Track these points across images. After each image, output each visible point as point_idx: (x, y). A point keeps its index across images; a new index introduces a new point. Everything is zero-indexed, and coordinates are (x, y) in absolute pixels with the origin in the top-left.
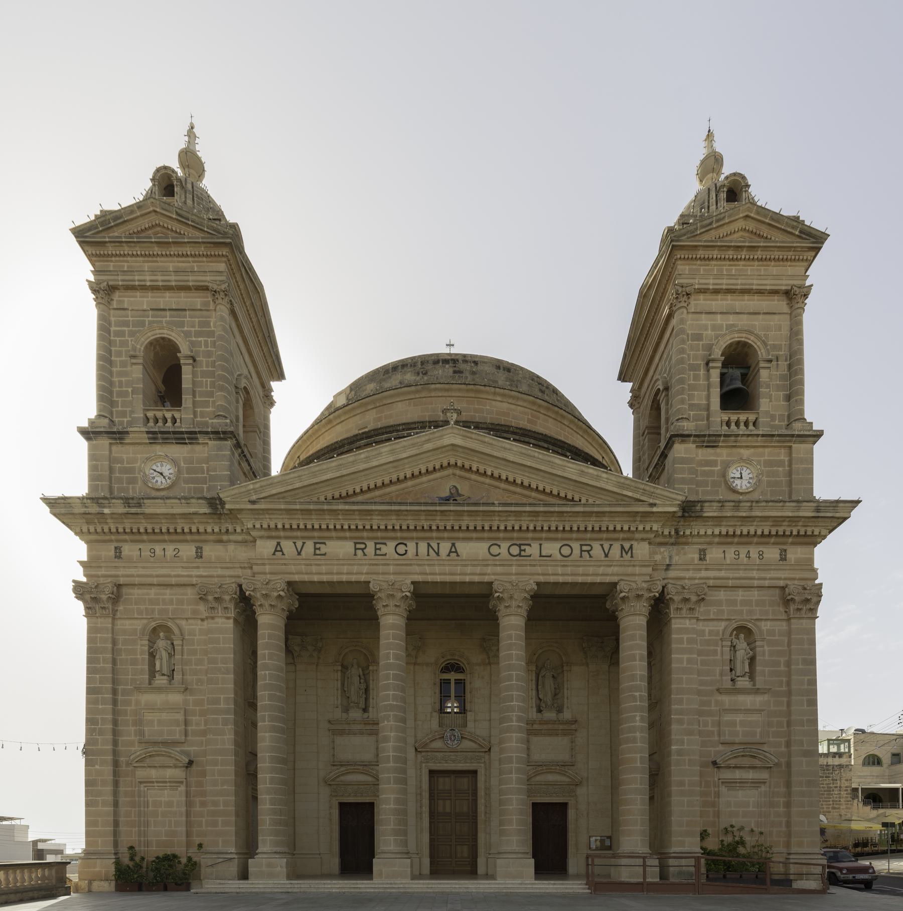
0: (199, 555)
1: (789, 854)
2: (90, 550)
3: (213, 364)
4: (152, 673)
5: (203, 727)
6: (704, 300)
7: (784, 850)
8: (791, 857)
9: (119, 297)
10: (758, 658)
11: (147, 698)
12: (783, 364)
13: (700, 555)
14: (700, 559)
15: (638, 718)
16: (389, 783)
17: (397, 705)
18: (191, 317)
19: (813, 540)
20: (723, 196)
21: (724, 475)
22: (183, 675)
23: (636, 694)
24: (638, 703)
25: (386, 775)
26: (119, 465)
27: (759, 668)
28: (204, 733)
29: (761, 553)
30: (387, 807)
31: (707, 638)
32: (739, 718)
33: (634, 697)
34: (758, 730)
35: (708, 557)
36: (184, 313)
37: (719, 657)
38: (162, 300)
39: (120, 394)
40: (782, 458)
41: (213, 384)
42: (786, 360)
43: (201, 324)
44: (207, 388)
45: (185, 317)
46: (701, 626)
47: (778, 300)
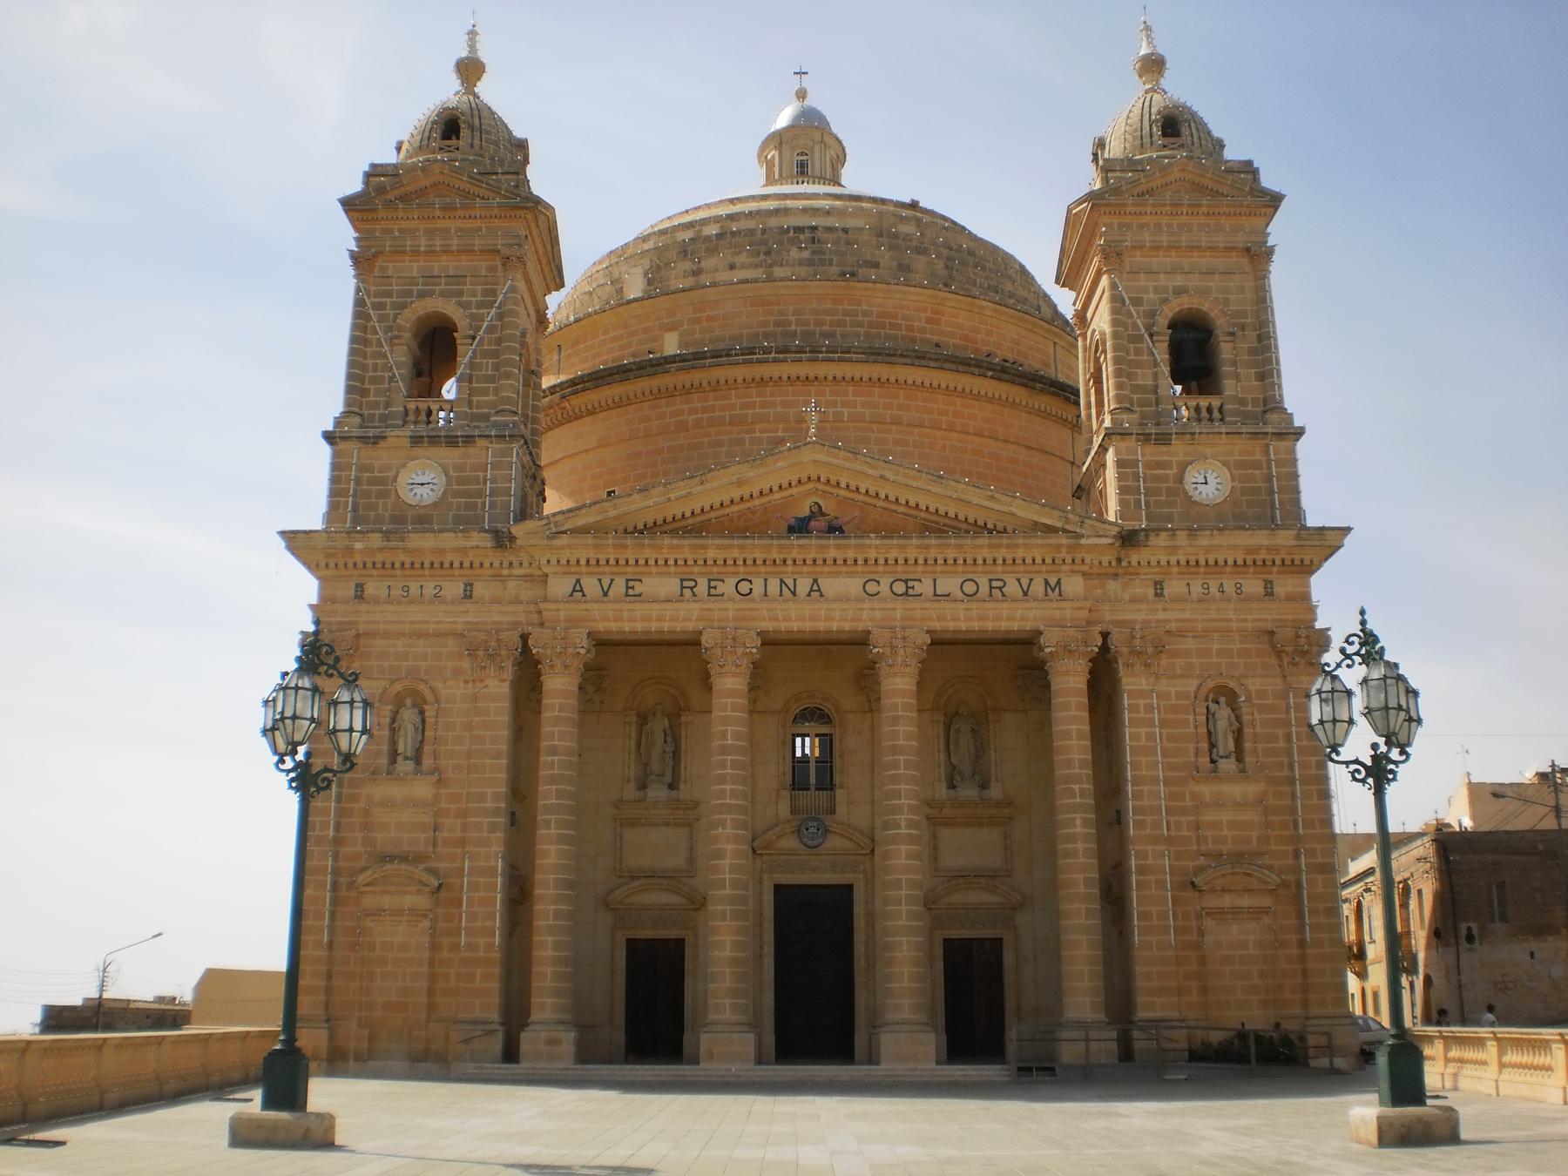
0: (468, 595)
1: (1308, 1019)
2: (322, 589)
3: (499, 341)
4: (394, 755)
5: (458, 834)
6: (1141, 257)
7: (1298, 1011)
8: (1309, 1023)
9: (384, 262)
10: (1246, 730)
11: (383, 790)
12: (1251, 334)
13: (1156, 589)
14: (1156, 595)
15: (1078, 822)
16: (724, 919)
17: (736, 805)
18: (473, 284)
19: (1309, 569)
20: (1157, 131)
21: (1180, 479)
22: (435, 758)
23: (1073, 786)
24: (1078, 800)
25: (719, 907)
26: (368, 474)
27: (1248, 745)
28: (462, 842)
29: (1238, 586)
30: (721, 954)
31: (1174, 702)
32: (1225, 816)
33: (1072, 791)
34: (1254, 834)
35: (1166, 592)
36: (464, 279)
37: (1192, 730)
38: (436, 264)
39: (374, 380)
40: (1258, 458)
41: (496, 367)
42: (1254, 330)
43: (486, 293)
44: (487, 370)
45: (465, 284)
46: (1163, 685)
47: (1237, 257)
